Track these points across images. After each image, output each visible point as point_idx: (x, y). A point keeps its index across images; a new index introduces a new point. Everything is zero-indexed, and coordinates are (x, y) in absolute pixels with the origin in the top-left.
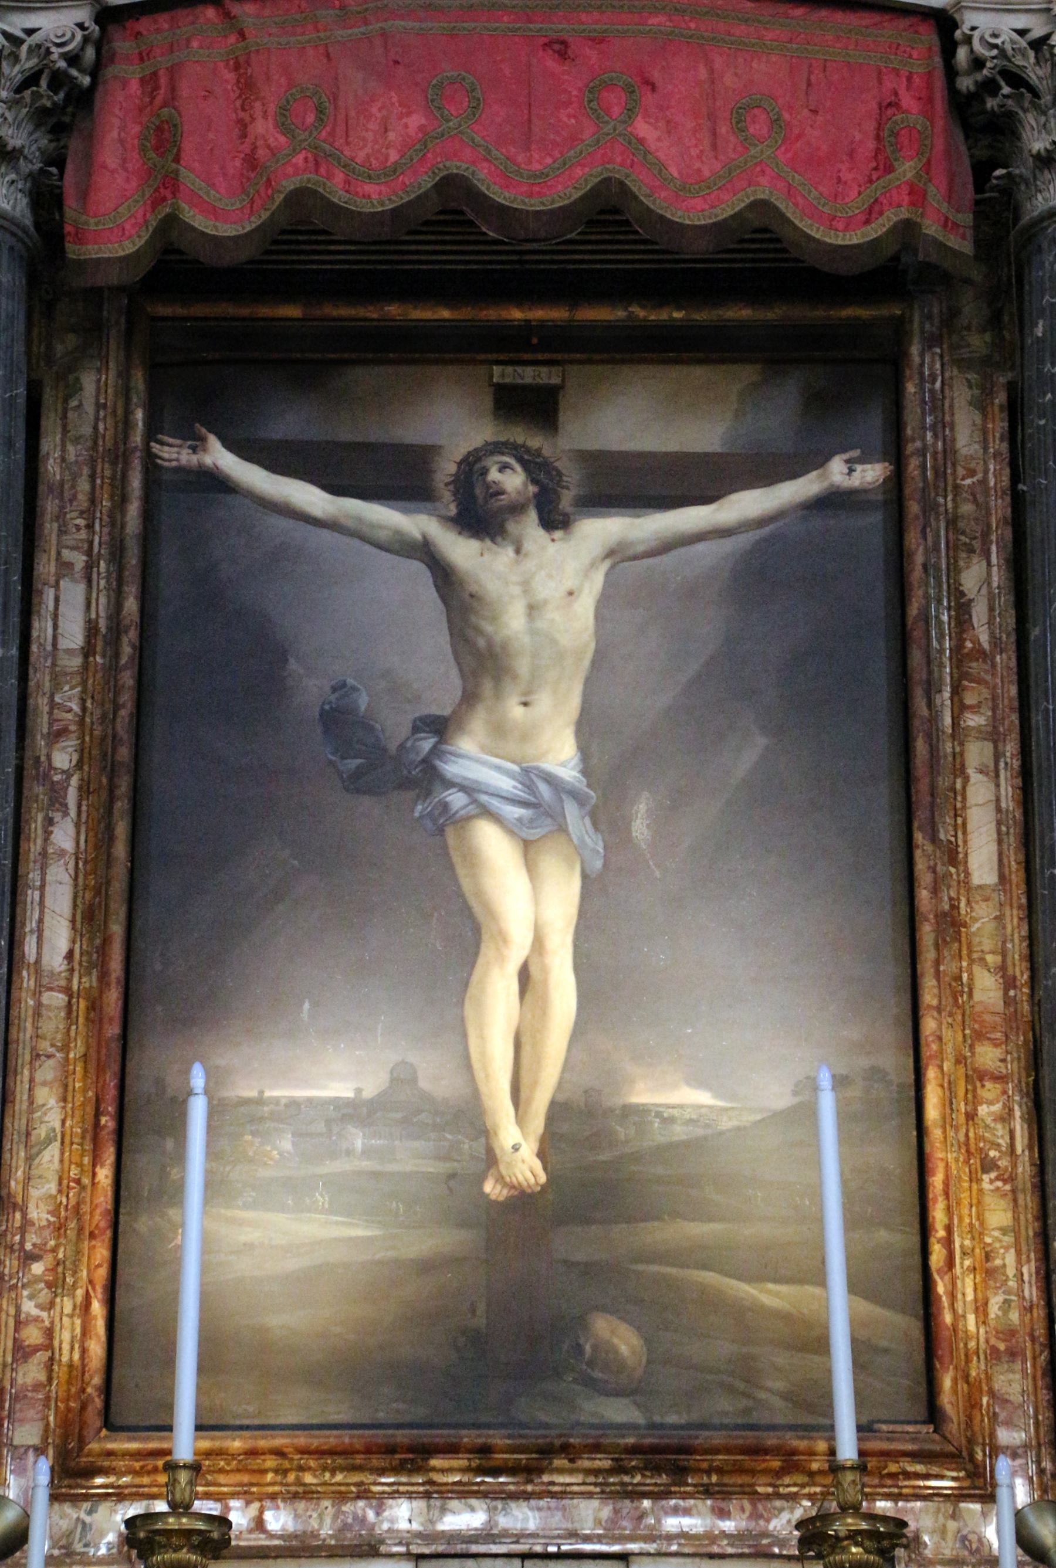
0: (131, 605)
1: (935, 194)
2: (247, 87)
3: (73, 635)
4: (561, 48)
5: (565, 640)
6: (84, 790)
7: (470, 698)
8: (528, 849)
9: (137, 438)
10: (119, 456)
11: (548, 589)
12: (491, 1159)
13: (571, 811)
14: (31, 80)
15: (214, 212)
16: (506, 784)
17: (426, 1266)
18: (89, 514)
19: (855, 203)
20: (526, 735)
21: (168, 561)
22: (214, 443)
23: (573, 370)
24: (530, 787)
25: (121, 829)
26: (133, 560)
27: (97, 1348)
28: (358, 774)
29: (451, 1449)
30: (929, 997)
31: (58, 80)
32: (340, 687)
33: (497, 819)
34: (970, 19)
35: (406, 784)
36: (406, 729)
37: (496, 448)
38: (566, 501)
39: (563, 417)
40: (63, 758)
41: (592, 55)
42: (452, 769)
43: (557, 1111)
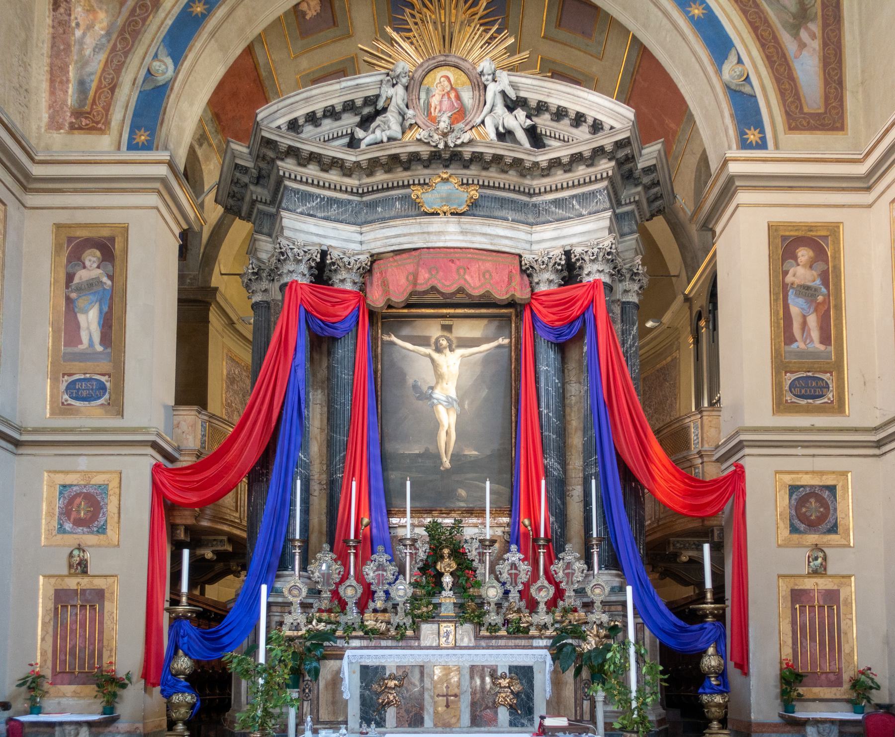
4: (452, 261)
9: (380, 335)
13: (455, 403)
14: (359, 268)
19: (504, 290)
21: (385, 358)
22: (393, 336)
23: (455, 322)
24: (448, 399)
28: (419, 396)
29: (436, 510)
31: (364, 268)
32: (415, 381)
33: (442, 405)
35: (427, 398)
39: (453, 330)
41: (458, 262)
43: (452, 455)
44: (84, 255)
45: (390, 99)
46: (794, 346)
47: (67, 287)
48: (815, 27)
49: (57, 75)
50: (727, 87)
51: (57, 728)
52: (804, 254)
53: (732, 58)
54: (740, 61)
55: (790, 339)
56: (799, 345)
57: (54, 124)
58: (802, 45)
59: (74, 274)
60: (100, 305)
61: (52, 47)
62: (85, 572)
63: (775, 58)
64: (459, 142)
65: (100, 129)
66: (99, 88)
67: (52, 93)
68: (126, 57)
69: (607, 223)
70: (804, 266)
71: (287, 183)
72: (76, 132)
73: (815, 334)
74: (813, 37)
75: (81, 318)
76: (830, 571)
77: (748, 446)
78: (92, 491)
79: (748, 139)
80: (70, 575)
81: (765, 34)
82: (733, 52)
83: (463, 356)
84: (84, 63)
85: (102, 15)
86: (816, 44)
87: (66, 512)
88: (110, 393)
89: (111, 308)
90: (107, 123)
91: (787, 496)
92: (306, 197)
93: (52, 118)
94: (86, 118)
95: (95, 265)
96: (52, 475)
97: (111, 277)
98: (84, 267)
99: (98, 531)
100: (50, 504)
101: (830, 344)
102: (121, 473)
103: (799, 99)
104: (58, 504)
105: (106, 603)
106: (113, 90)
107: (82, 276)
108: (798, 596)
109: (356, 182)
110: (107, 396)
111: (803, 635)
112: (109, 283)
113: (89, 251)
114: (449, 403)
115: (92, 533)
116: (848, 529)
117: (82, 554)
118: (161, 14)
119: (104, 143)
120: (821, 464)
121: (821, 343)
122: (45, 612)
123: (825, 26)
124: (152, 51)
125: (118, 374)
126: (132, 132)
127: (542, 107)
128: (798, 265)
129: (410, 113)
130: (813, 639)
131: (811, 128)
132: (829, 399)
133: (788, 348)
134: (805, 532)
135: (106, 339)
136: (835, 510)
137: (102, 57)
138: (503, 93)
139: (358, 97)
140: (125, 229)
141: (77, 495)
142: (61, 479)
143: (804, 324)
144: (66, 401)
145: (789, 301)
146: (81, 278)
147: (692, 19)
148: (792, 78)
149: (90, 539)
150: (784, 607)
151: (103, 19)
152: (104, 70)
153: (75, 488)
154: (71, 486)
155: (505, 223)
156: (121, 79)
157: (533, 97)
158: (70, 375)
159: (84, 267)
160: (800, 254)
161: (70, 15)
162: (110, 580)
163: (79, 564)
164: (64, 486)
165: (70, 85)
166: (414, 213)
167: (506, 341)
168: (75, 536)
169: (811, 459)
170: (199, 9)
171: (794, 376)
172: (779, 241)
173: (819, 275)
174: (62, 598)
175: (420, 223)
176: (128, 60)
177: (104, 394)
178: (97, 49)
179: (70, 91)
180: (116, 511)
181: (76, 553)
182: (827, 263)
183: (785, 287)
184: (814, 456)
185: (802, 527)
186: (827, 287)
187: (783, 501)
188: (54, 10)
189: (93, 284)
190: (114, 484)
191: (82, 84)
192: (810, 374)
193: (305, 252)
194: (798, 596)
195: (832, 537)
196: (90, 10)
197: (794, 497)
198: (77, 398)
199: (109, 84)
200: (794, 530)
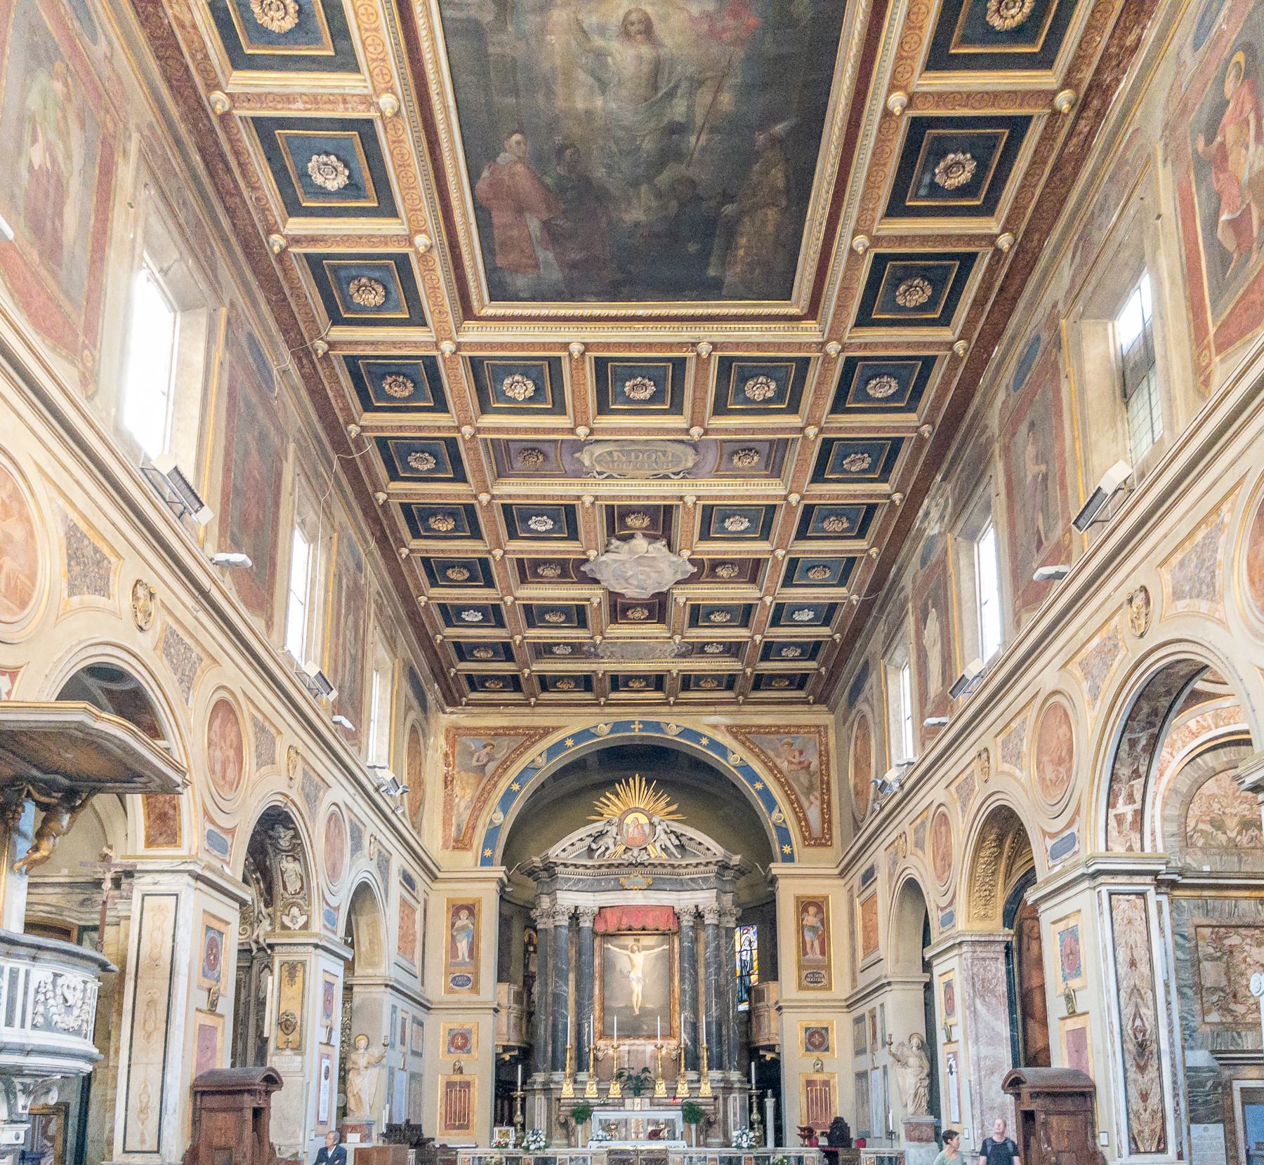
48: (817, 794)
49: (446, 823)
84: (460, 815)
86: (818, 803)
114: (638, 981)
118: (497, 790)
137: (469, 812)
139: (593, 832)
148: (806, 820)
151: (469, 793)
157: (679, 831)
170: (516, 787)
178: (466, 808)
191: (458, 825)
196: (463, 788)
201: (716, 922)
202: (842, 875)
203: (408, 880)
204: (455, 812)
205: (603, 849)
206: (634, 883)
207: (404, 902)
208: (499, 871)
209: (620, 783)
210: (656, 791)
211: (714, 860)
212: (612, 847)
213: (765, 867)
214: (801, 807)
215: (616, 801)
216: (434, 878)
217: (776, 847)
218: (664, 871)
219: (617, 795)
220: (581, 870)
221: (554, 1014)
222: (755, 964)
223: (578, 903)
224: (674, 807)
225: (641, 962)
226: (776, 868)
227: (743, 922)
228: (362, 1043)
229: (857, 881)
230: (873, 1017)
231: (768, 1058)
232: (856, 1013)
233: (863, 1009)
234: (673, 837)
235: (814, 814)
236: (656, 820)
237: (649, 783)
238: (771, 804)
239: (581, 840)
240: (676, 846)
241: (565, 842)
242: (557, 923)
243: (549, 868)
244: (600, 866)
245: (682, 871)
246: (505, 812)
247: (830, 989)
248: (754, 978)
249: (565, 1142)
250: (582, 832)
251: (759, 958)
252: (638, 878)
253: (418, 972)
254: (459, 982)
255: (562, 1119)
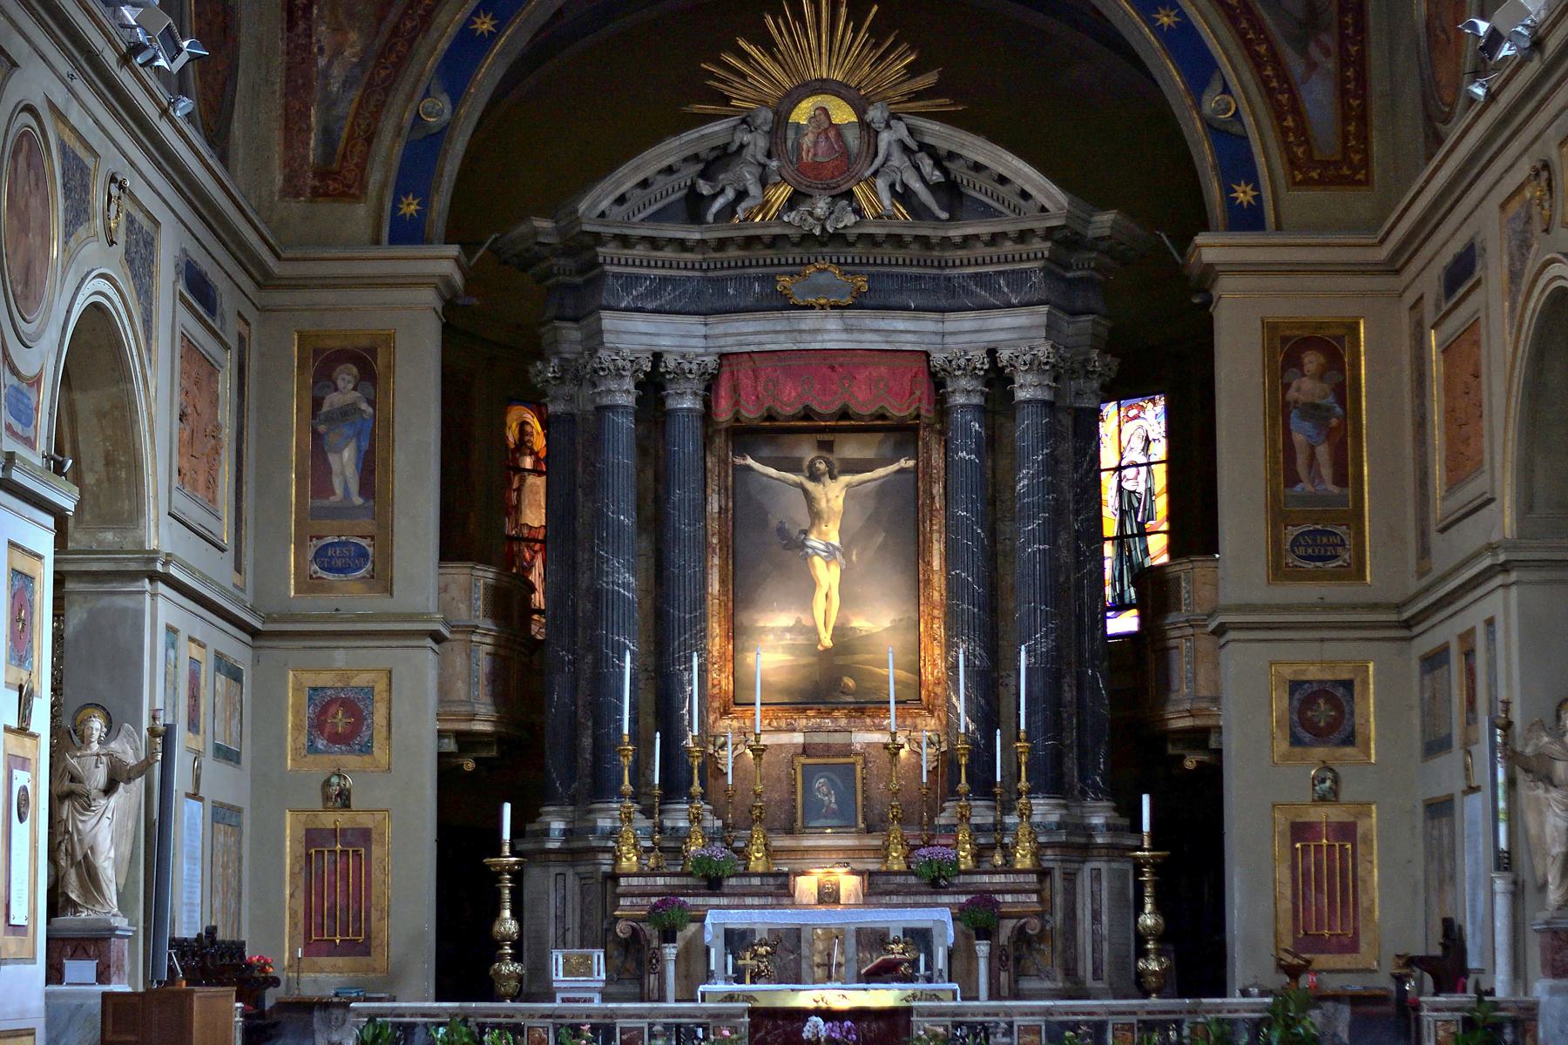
0: (730, 504)
1: (924, 402)
2: (756, 378)
3: (716, 509)
5: (836, 509)
6: (721, 549)
7: (813, 525)
8: (827, 563)
10: (726, 463)
11: (831, 495)
12: (819, 641)
15: (750, 412)
16: (822, 547)
17: (804, 666)
18: (719, 476)
20: (827, 534)
25: (730, 562)
26: (730, 493)
27: (731, 687)
30: (922, 602)
34: (933, 355)
36: (797, 531)
37: (818, 457)
38: (836, 471)
40: (715, 541)
42: (809, 543)
44: (335, 374)
45: (742, 146)
46: (1299, 488)
47: (314, 416)
48: (1329, 40)
49: (293, 123)
50: (1209, 125)
51: (317, 1015)
52: (1312, 360)
53: (1217, 86)
54: (1226, 90)
55: (1292, 479)
56: (1305, 487)
57: (292, 189)
58: (1312, 66)
59: (323, 399)
60: (359, 441)
61: (287, 82)
62: (346, 806)
63: (1274, 84)
64: (841, 225)
65: (353, 196)
66: (351, 137)
67: (288, 145)
68: (387, 95)
69: (1044, 320)
70: (1312, 377)
71: (608, 268)
72: (320, 199)
73: (1326, 472)
74: (1327, 52)
75: (333, 459)
76: (1343, 796)
77: (1234, 629)
78: (351, 695)
79: (1237, 198)
80: (326, 809)
81: (1262, 49)
82: (1217, 76)
83: (848, 486)
84: (329, 104)
85: (353, 36)
86: (1330, 64)
87: (318, 724)
88: (373, 562)
89: (372, 445)
90: (363, 186)
91: (1286, 696)
92: (634, 280)
93: (288, 180)
94: (335, 180)
95: (351, 386)
96: (299, 674)
97: (372, 403)
98: (336, 389)
99: (360, 750)
100: (296, 713)
101: (1346, 485)
102: (390, 672)
103: (1307, 142)
104: (308, 713)
105: (373, 847)
106: (369, 141)
107: (333, 401)
108: (1301, 831)
109: (700, 257)
110: (369, 566)
111: (1306, 882)
112: (370, 410)
113: (342, 367)
115: (352, 752)
116: (1369, 739)
117: (343, 782)
119: (359, 214)
120: (1332, 650)
121: (1335, 483)
122: (294, 859)
123: (1343, 37)
124: (422, 88)
125: (384, 535)
126: (396, 201)
127: (952, 156)
128: (1304, 375)
129: (774, 164)
130: (1319, 888)
131: (1322, 182)
132: (1344, 561)
133: (1288, 491)
134: (1311, 745)
135: (367, 488)
136: (1352, 713)
137: (355, 94)
138: (901, 142)
139: (703, 149)
140: (388, 340)
141: (331, 702)
142: (312, 680)
143: (1312, 456)
144: (316, 572)
145: (1292, 427)
146: (332, 405)
147: (1158, 31)
148: (1296, 109)
149: (351, 761)
150: (1279, 847)
152: (357, 114)
153: (329, 693)
154: (323, 688)
155: (906, 314)
156: (380, 125)
157: (943, 146)
158: (319, 538)
159: (336, 389)
160: (1306, 360)
161: (310, 36)
162: (379, 816)
163: (339, 795)
164: (315, 689)
165: (313, 135)
166: (779, 304)
167: (911, 463)
168: (332, 757)
169: (1317, 644)
170: (485, 25)
171: (1297, 531)
172: (1278, 342)
173: (1333, 390)
174: (314, 838)
175: (788, 318)
176: (390, 99)
177: (365, 564)
178: (347, 84)
179: (312, 143)
180: (384, 723)
181: (335, 780)
182: (1342, 371)
183: (1286, 408)
184: (1322, 640)
185: (1307, 737)
186: (1342, 403)
187: (1280, 703)
188: (290, 29)
189: (347, 412)
190: (381, 687)
191: (328, 135)
192: (1319, 527)
193: (632, 361)
194: (1301, 831)
195: (1349, 750)
196: (337, 29)
197: (1297, 696)
198: (329, 569)
199: (366, 132)
200: (1295, 741)
201: (1045, 395)
202: (1392, 268)
203: (198, 288)
204: (317, 95)
205: (730, 194)
206: (818, 291)
207: (190, 348)
208: (443, 261)
209: (777, 13)
210: (877, 33)
211: (1040, 225)
212: (754, 189)
213: (1184, 240)
214: (1284, 77)
215: (767, 63)
216: (266, 281)
217: (1213, 189)
218: (900, 254)
219: (768, 45)
220: (668, 254)
221: (594, 646)
222: (1161, 505)
223: (664, 343)
224: (928, 80)
225: (838, 504)
226: (1211, 248)
227: (1126, 388)
228: (97, 725)
229: (1431, 283)
230: (1469, 654)
231: (1190, 764)
232: (1427, 643)
233: (1445, 632)
234: (927, 164)
235: (1318, 96)
236: (875, 114)
237: (856, 16)
238: (1200, 68)
239: (669, 170)
240: (933, 188)
241: (626, 178)
242: (606, 401)
243: (582, 246)
244: (722, 244)
245: (948, 254)
246: (456, 98)
247: (1360, 574)
248: (1157, 545)
249: (633, 989)
250: (671, 150)
251: (1171, 488)
252: (827, 275)
253: (226, 538)
254: (338, 559)
255: (622, 929)
